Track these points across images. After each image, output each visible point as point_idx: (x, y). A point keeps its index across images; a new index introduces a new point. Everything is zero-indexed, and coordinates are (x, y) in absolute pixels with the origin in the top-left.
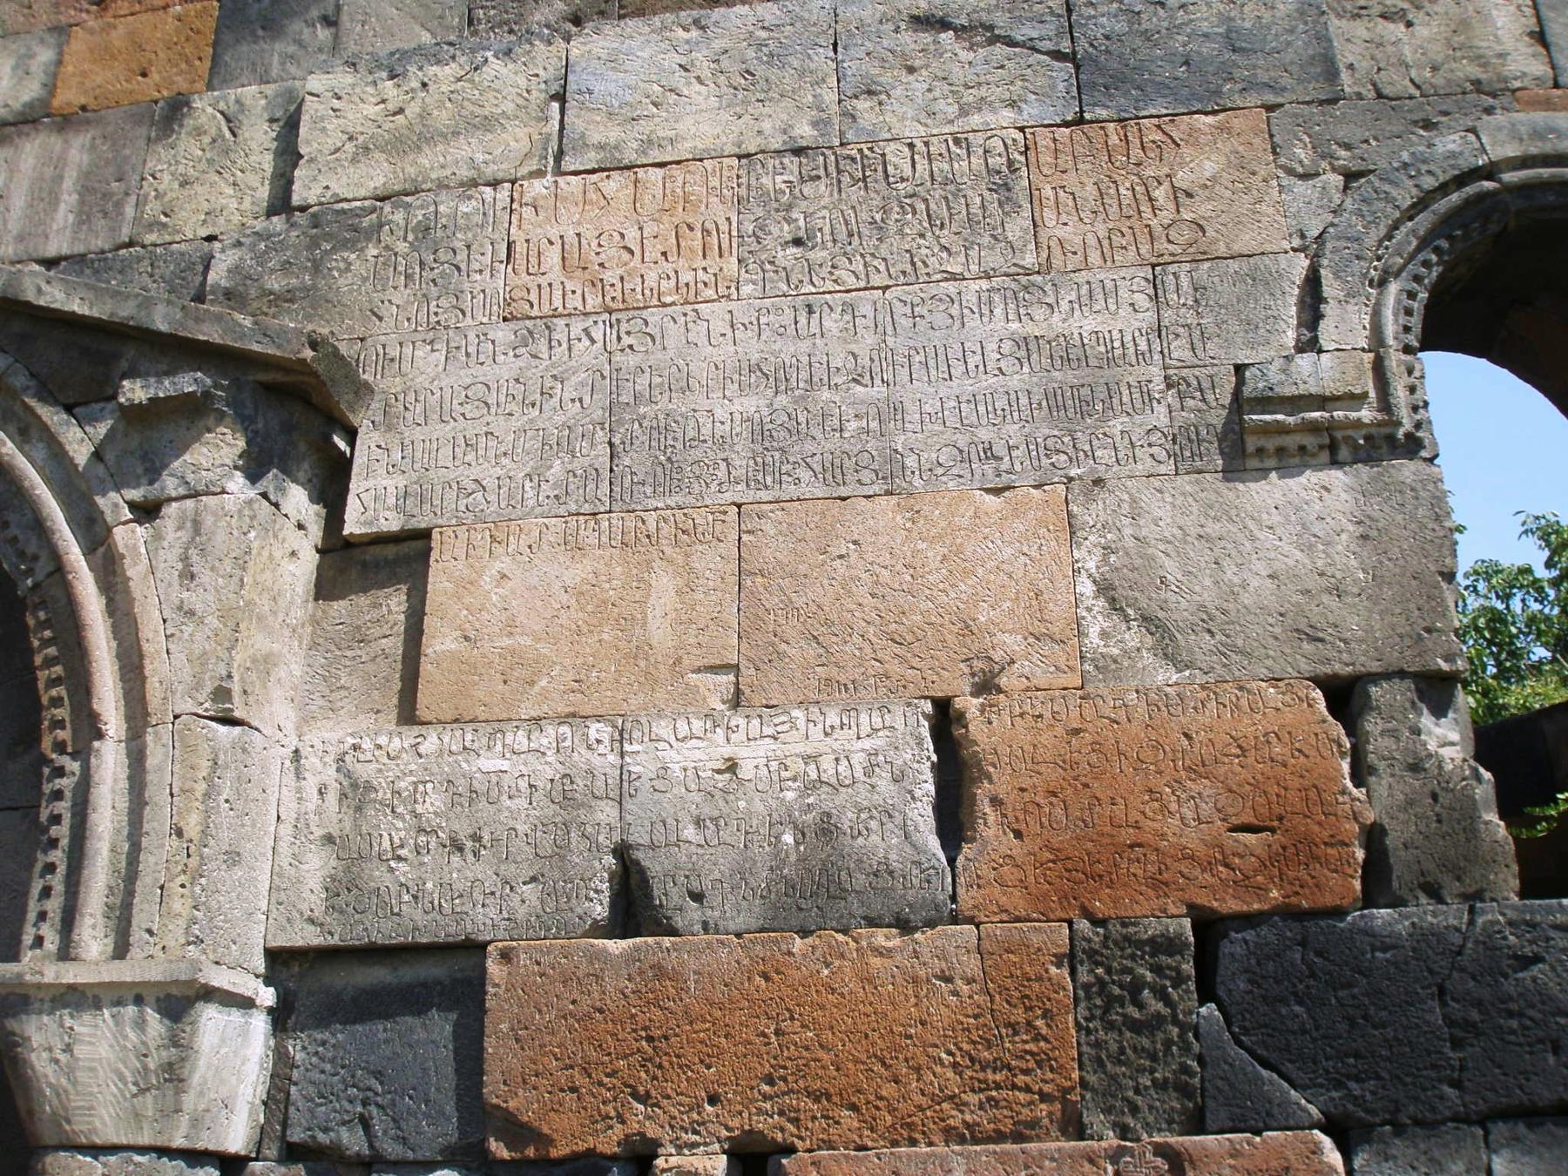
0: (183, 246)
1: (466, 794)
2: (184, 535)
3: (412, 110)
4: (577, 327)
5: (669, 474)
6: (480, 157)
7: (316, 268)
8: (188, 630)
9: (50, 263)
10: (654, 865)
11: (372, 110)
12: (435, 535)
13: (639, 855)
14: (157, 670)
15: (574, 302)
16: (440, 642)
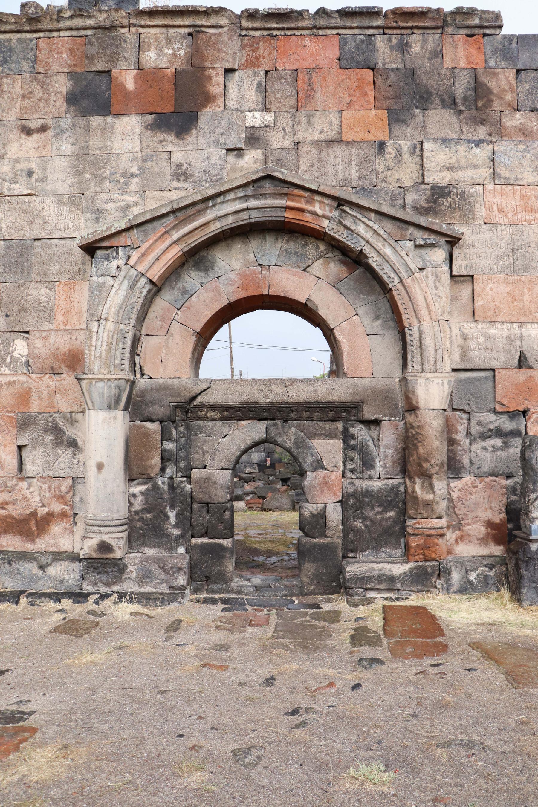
0: (393, 189)
1: (489, 338)
2: (434, 278)
3: (454, 158)
4: (503, 227)
5: (526, 268)
6: (474, 176)
7: (435, 202)
8: (439, 300)
9: (353, 188)
10: (528, 355)
11: (443, 157)
12: (475, 277)
13: (525, 352)
14: (432, 308)
15: (501, 221)
16: (479, 303)
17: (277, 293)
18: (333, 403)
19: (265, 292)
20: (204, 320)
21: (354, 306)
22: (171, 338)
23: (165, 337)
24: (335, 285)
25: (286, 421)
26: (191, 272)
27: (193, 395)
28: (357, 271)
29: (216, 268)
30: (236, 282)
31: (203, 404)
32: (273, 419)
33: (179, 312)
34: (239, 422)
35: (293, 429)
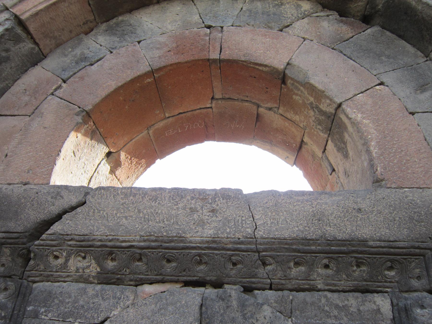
17: (235, 57)
18: (363, 242)
19: (214, 55)
20: (103, 93)
21: (375, 73)
22: (39, 119)
23: (27, 118)
24: (336, 45)
25: (248, 290)
26: (99, 37)
27: (43, 216)
28: (369, 30)
29: (139, 31)
30: (167, 45)
31: (63, 239)
32: (218, 285)
33: (64, 85)
34: (139, 288)
35: (267, 311)
